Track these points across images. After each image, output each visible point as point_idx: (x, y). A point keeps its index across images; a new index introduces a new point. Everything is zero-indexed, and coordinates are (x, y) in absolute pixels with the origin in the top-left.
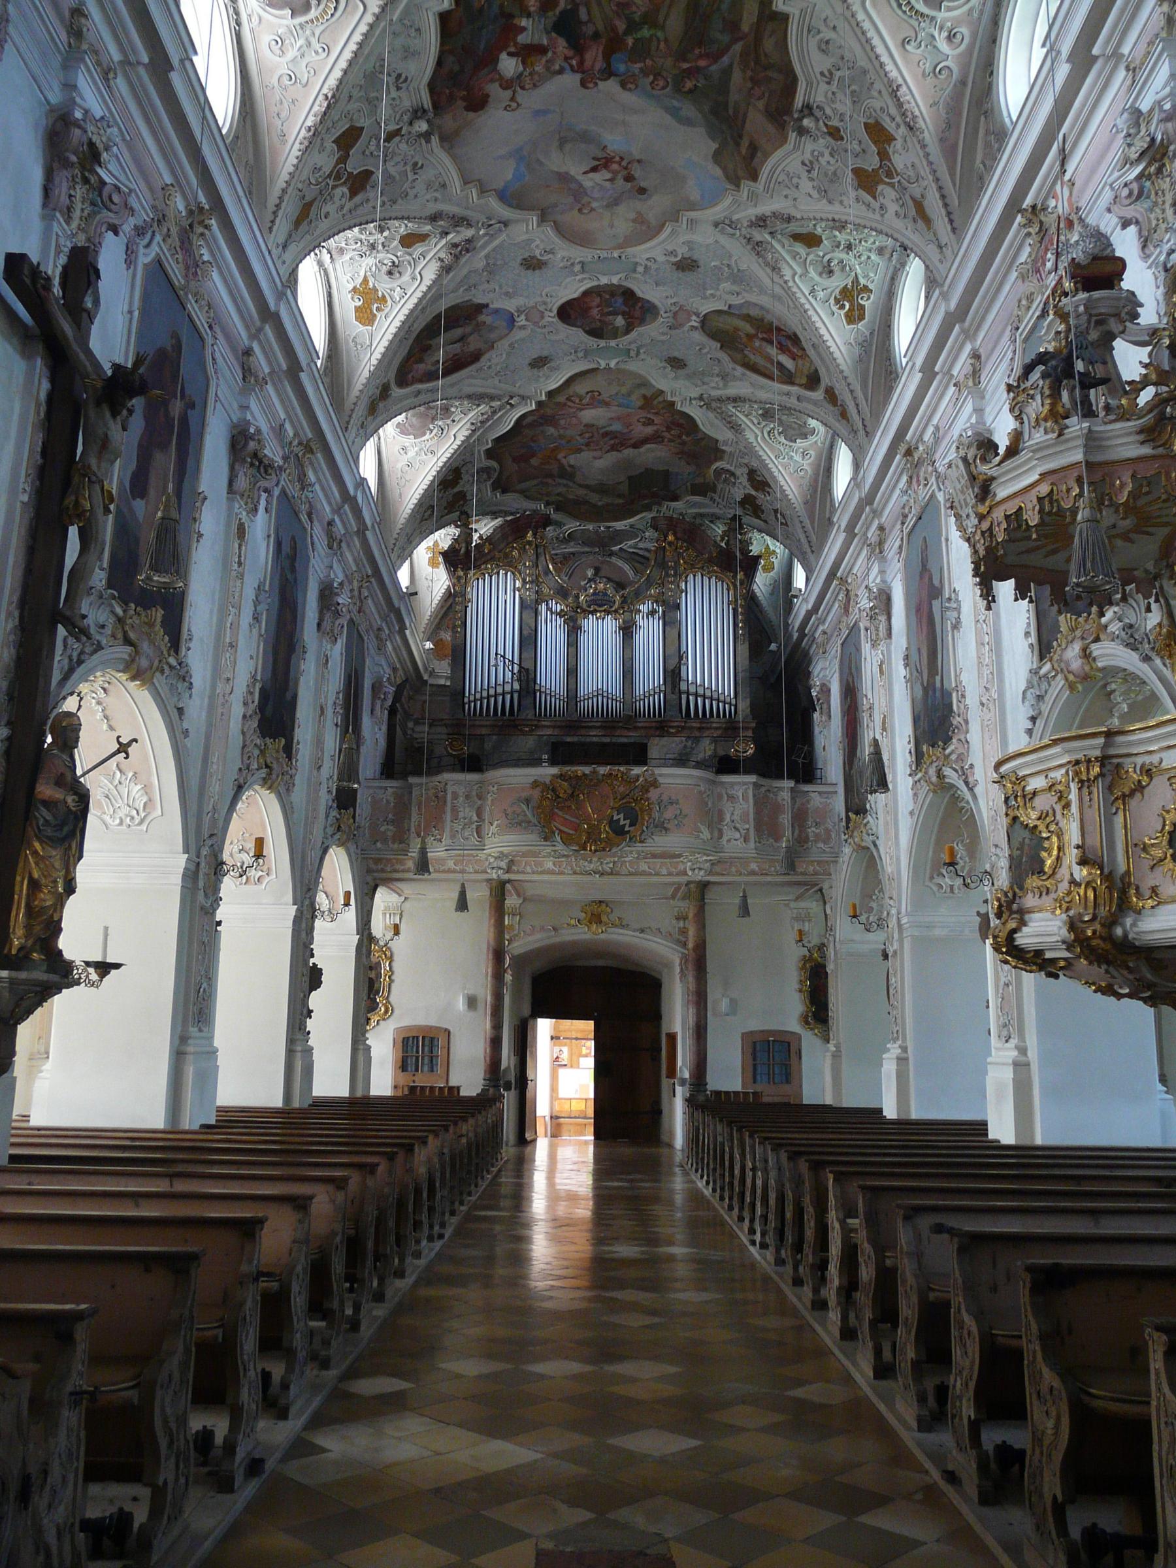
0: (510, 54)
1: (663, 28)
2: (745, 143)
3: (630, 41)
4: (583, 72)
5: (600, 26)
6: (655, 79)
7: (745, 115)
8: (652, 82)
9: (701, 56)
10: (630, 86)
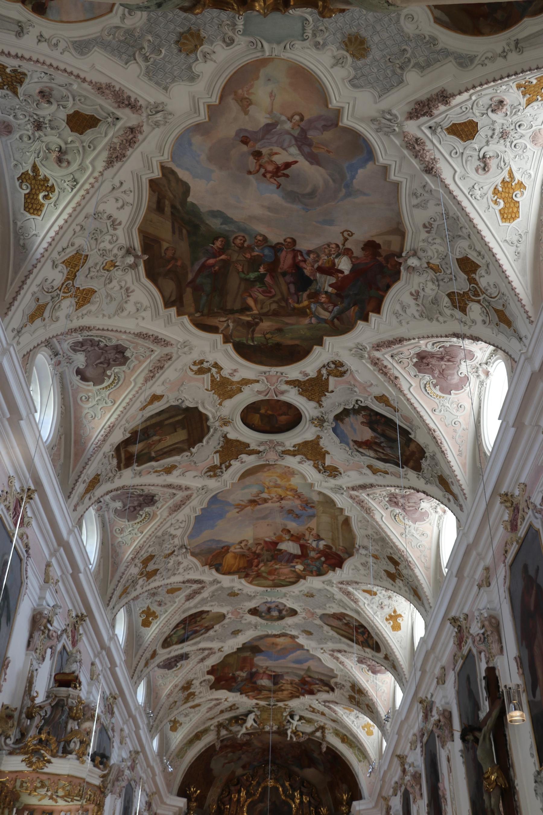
0: (342, 272)
1: (242, 279)
2: (168, 209)
3: (262, 270)
4: (294, 250)
5: (281, 280)
6: (243, 244)
7: (174, 232)
8: (245, 241)
9: (213, 266)
10: (260, 238)
